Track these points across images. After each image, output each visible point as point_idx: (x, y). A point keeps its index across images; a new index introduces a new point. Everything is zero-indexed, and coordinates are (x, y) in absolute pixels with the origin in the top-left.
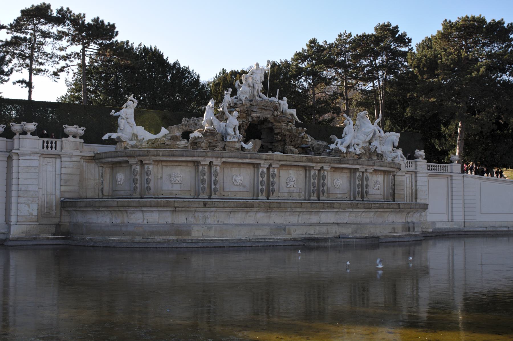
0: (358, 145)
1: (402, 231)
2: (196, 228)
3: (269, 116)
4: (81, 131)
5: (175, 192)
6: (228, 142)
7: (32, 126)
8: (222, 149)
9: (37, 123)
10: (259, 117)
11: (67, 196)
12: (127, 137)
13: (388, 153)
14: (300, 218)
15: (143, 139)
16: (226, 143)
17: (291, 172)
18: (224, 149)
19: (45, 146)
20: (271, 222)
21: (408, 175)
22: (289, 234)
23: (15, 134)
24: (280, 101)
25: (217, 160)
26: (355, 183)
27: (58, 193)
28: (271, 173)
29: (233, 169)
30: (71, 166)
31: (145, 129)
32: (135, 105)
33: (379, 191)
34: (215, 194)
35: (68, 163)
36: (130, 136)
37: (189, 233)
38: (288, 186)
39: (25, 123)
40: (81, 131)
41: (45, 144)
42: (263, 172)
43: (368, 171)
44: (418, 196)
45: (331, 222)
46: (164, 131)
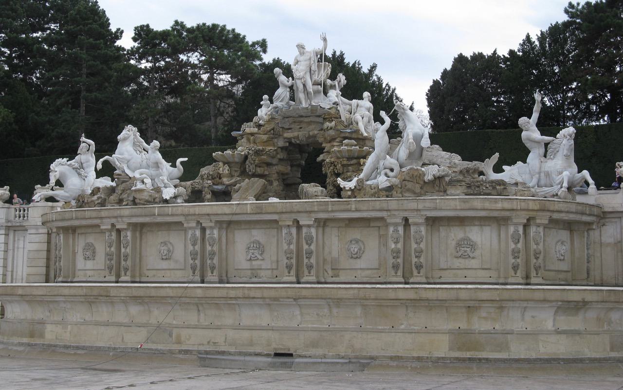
0: (392, 170)
1: (451, 349)
2: (49, 327)
3: (316, 132)
5: (89, 273)
6: (136, 191)
9: (8, 187)
10: (298, 137)
12: (67, 194)
13: (555, 177)
14: (202, 315)
16: (133, 194)
18: (134, 202)
20: (153, 321)
22: (179, 342)
24: (355, 102)
25: (118, 222)
26: (386, 245)
29: (160, 233)
30: (37, 240)
32: (93, 148)
33: (473, 261)
34: (125, 274)
37: (42, 336)
38: (249, 258)
42: (194, 235)
43: (410, 221)
45: (264, 324)
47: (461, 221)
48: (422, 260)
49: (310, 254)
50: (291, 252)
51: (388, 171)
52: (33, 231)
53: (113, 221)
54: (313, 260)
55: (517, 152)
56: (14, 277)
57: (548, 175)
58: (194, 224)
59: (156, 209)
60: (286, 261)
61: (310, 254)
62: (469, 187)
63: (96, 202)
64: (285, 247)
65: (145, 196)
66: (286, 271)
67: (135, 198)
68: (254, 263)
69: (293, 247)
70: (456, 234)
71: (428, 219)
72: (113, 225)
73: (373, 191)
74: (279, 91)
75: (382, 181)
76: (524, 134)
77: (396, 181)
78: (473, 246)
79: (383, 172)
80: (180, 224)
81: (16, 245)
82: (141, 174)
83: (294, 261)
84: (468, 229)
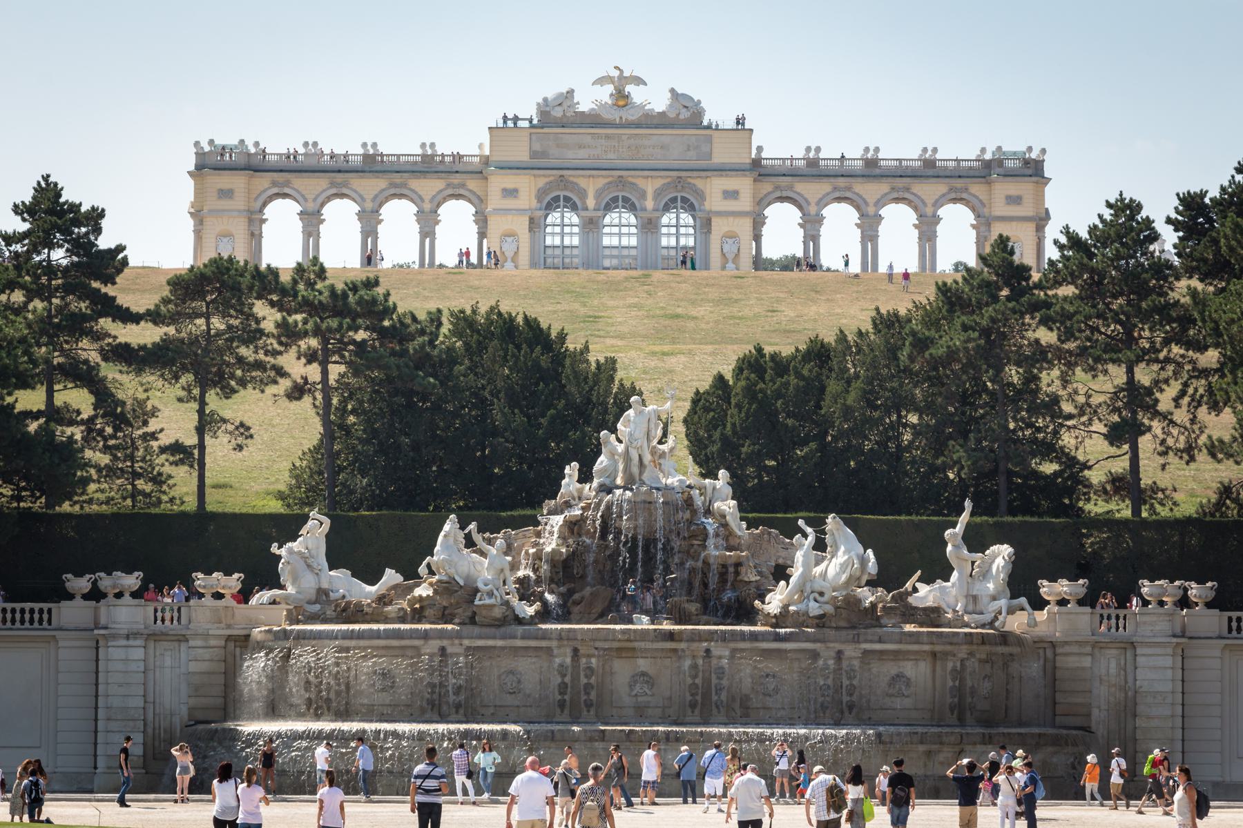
4: (234, 581)
7: (132, 581)
8: (467, 621)
11: (200, 715)
12: (300, 596)
15: (344, 597)
17: (641, 662)
18: (472, 621)
19: (159, 618)
21: (1114, 652)
23: (104, 596)
25: (453, 645)
27: (184, 710)
28: (582, 666)
30: (207, 657)
31: (353, 576)
35: (200, 651)
36: (312, 595)
39: (119, 573)
40: (234, 581)
41: (159, 614)
44: (1141, 709)
46: (391, 577)
47: (897, 656)
48: (854, 698)
49: (719, 690)
50: (696, 686)
51: (817, 595)
52: (199, 643)
53: (445, 643)
54: (724, 696)
55: (939, 570)
56: (157, 711)
57: (975, 598)
58: (569, 651)
59: (520, 630)
60: (689, 698)
61: (719, 690)
62: (903, 615)
63: (393, 615)
64: (689, 681)
65: (498, 613)
66: (689, 711)
67: (475, 613)
68: (640, 699)
69: (698, 681)
70: (891, 669)
71: (866, 652)
72: (443, 649)
73: (801, 619)
74: (602, 461)
75: (814, 609)
76: (949, 548)
77: (829, 609)
78: (908, 683)
79: (811, 597)
80: (549, 649)
81: (158, 663)
82: (486, 585)
83: (699, 698)
84: (902, 663)
